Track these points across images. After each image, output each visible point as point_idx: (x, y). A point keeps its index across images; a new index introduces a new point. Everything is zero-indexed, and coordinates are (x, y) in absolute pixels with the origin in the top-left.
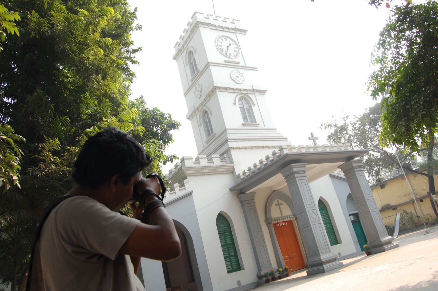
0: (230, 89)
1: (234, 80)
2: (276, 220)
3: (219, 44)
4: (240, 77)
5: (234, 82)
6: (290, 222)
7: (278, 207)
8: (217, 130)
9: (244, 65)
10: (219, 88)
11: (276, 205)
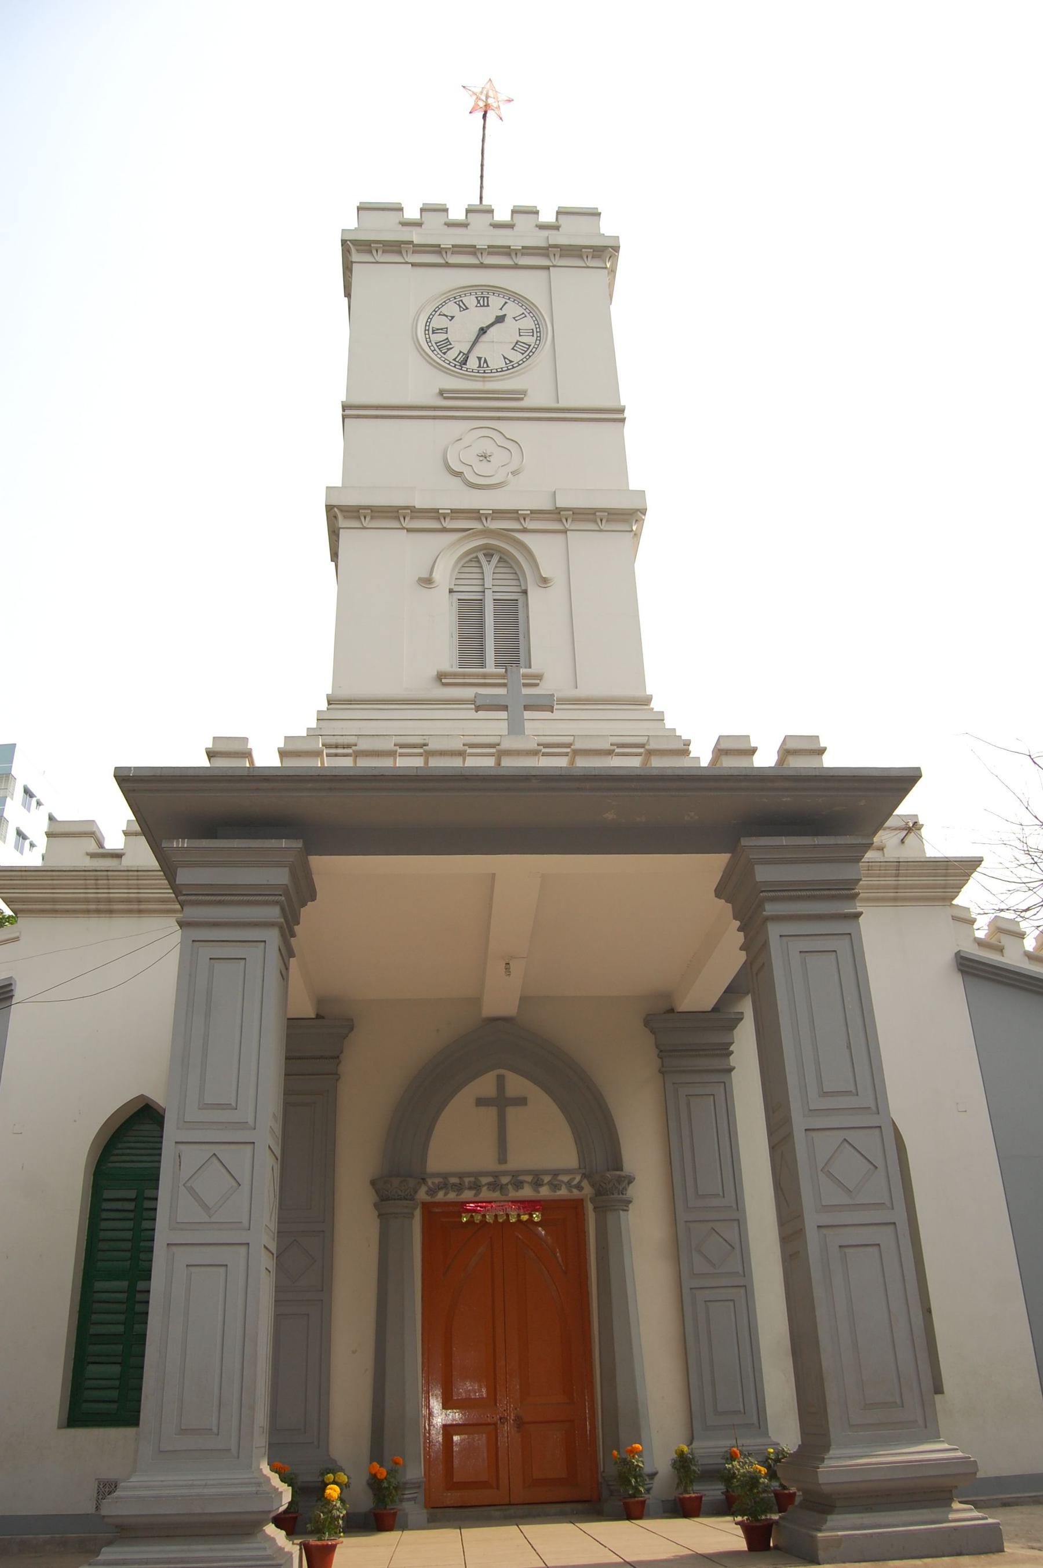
0: (415, 512)
1: (458, 474)
2: (445, 1186)
3: (438, 322)
4: (499, 457)
5: (457, 481)
6: (576, 1206)
7: (492, 1112)
9: (553, 405)
11: (481, 1102)
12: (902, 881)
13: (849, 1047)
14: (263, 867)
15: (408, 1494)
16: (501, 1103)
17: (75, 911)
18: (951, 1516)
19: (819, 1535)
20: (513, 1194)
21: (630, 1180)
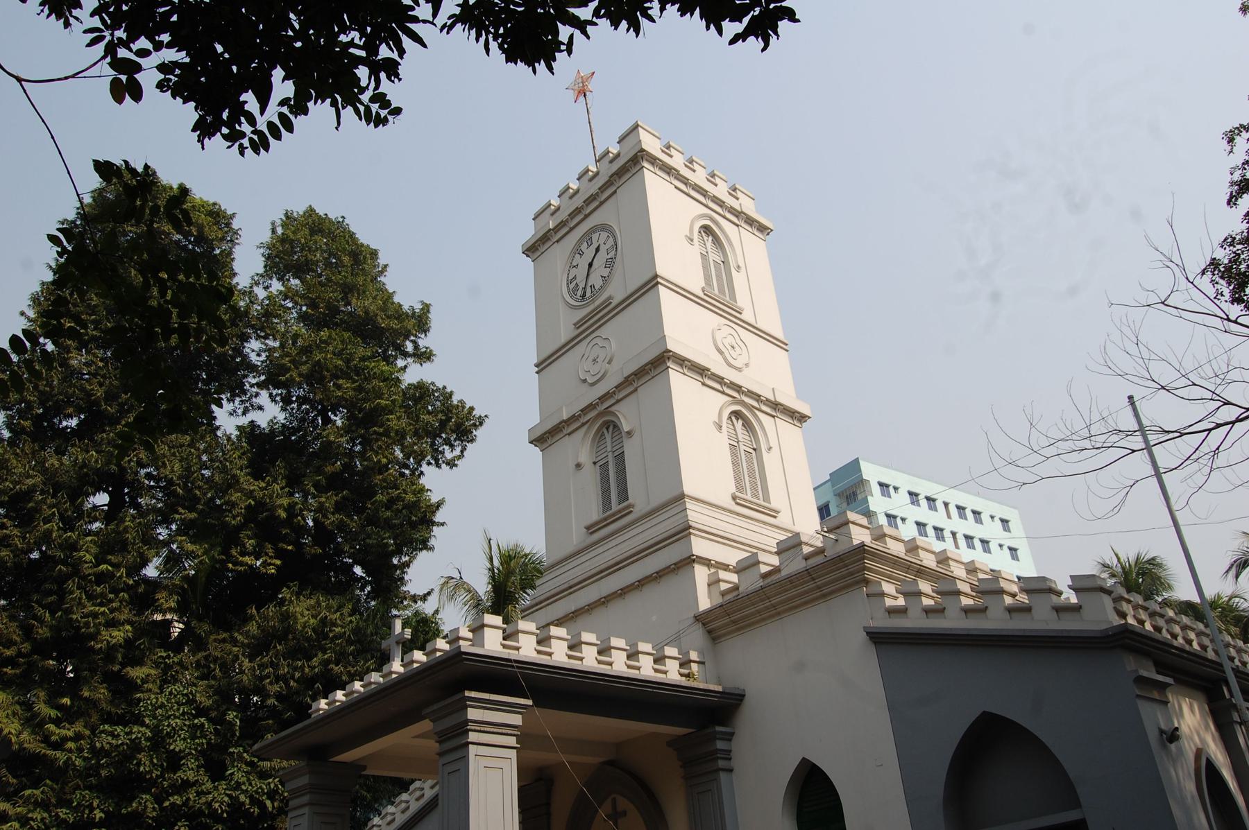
8: (639, 499)
9: (752, 321)
10: (682, 361)
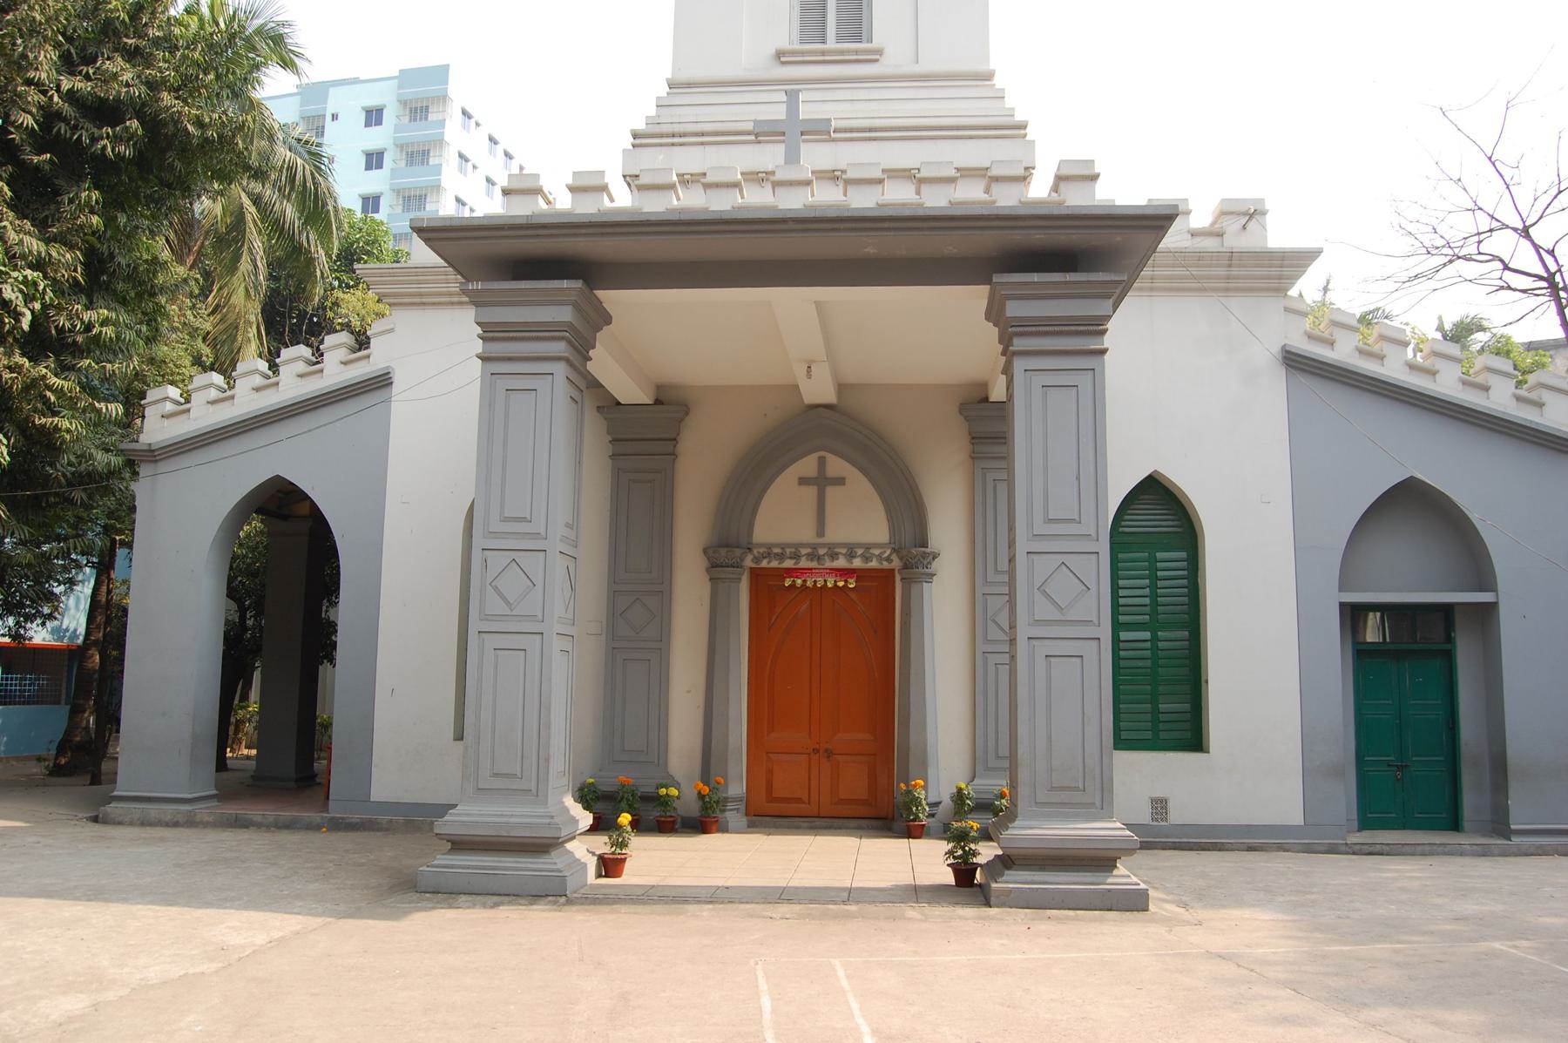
2: (768, 555)
6: (886, 577)
7: (811, 492)
11: (803, 481)
12: (1235, 272)
13: (1078, 478)
14: (552, 304)
15: (730, 806)
16: (821, 482)
17: (440, 304)
18: (1110, 880)
19: (994, 885)
20: (829, 564)
21: (935, 556)
